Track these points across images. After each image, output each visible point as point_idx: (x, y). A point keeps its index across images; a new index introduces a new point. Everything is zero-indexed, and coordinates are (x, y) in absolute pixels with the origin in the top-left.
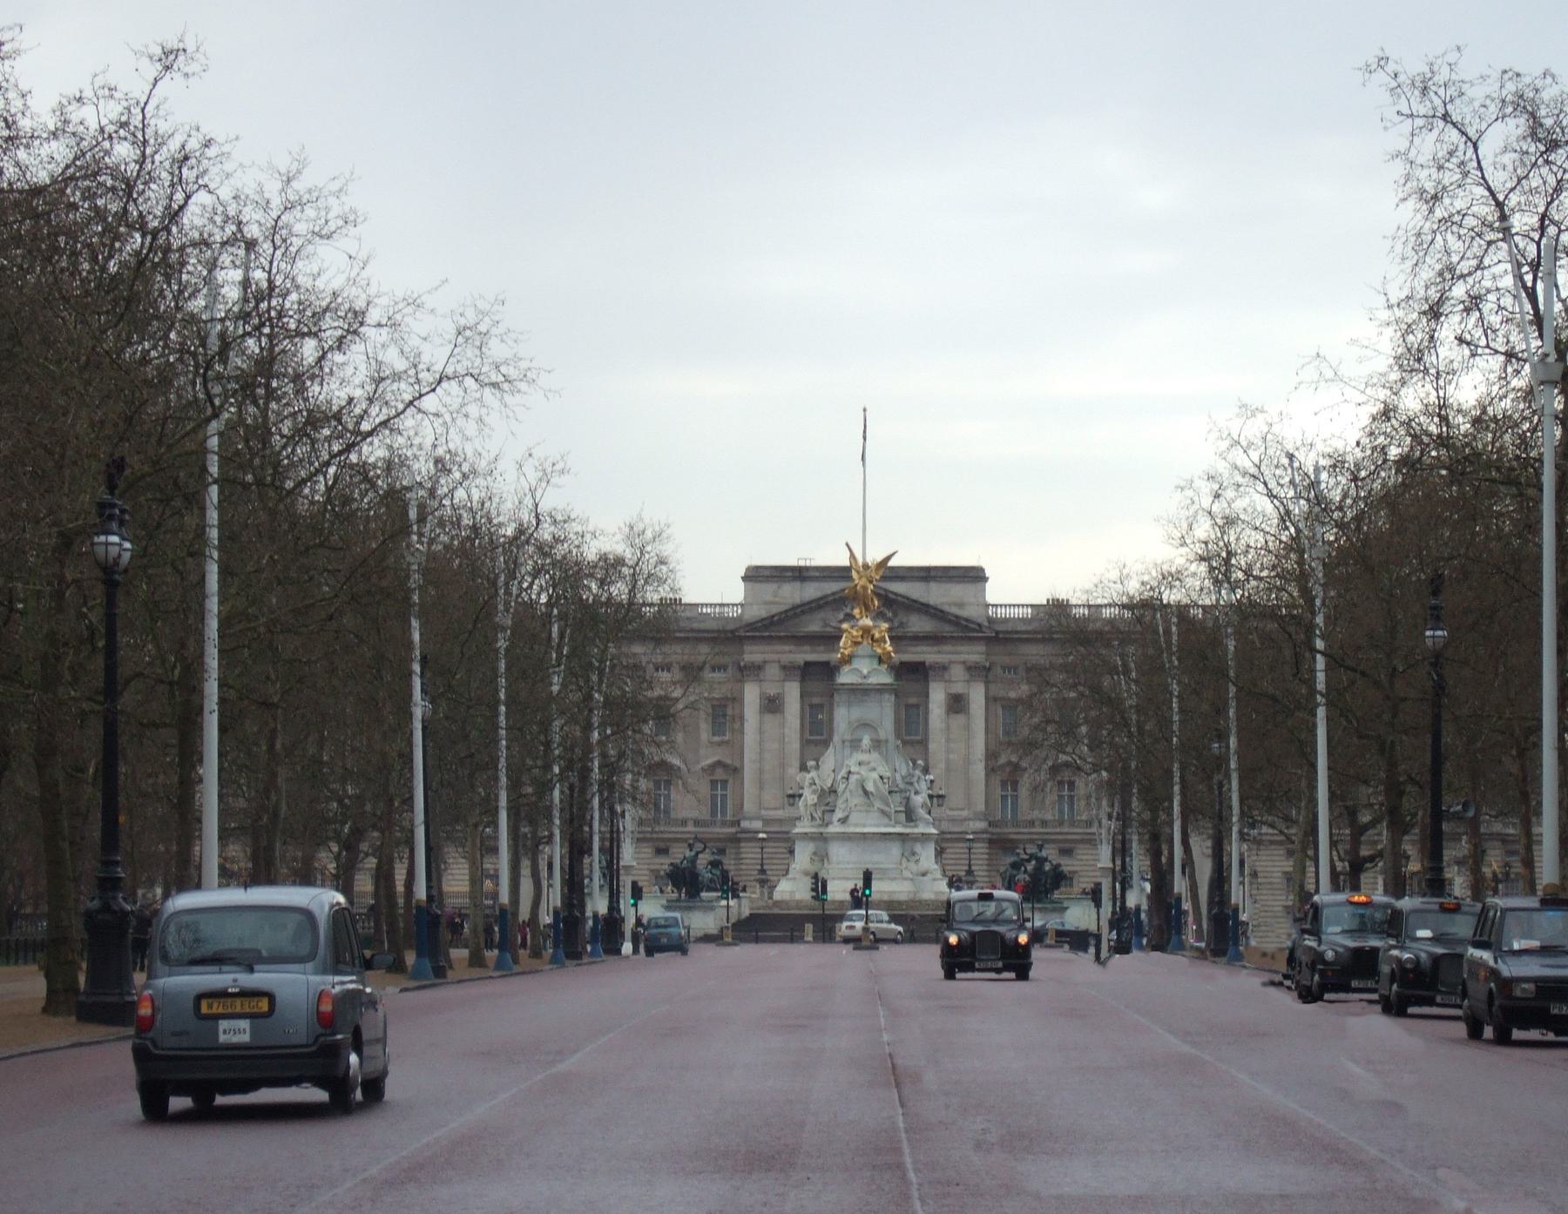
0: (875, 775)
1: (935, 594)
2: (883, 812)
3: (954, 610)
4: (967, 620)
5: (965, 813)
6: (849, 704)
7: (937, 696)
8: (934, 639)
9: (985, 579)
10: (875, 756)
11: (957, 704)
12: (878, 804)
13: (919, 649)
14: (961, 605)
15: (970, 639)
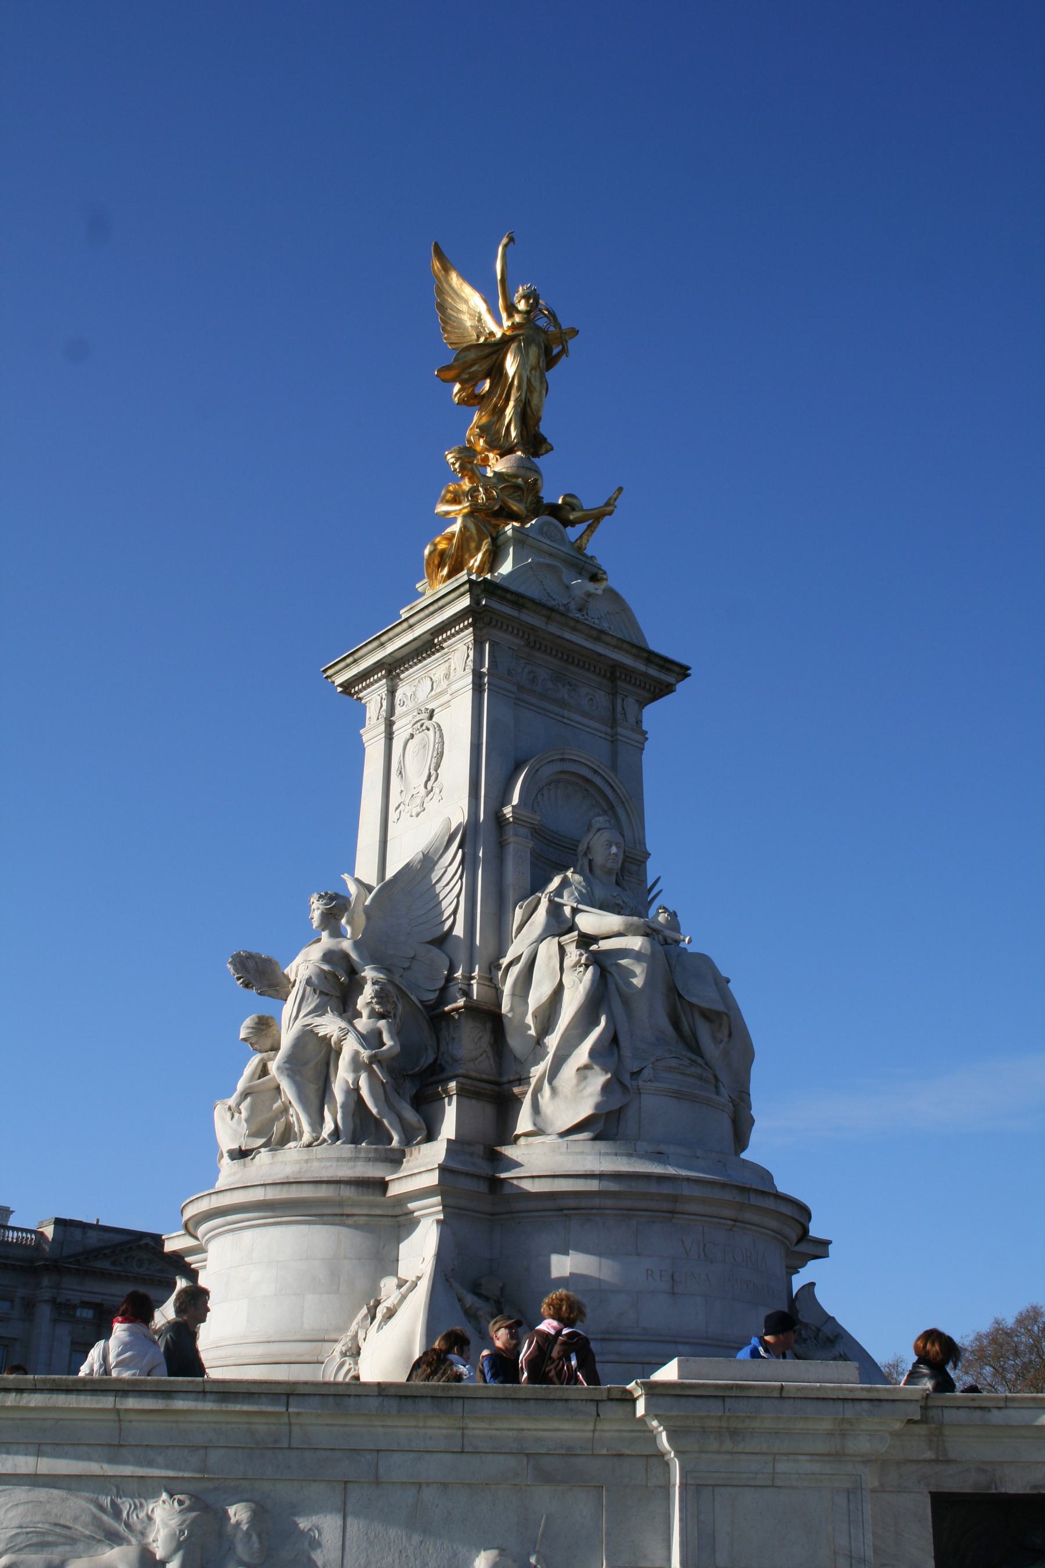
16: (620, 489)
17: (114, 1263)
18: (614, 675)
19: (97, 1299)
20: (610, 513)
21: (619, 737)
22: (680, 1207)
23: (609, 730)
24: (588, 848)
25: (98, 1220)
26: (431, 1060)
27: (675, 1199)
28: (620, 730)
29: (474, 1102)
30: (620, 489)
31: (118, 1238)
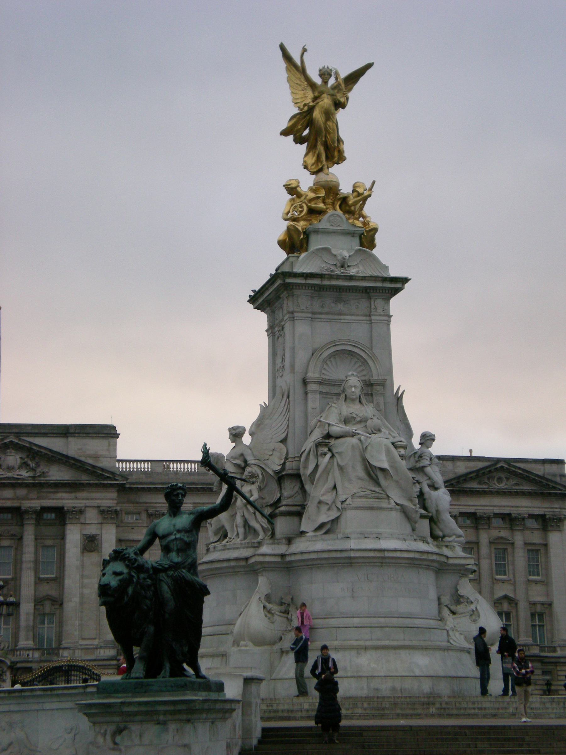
0: (381, 440)
1: (72, 447)
2: (404, 511)
3: (90, 461)
4: (103, 470)
5: (96, 642)
6: (314, 316)
7: (74, 536)
8: (72, 487)
9: (117, 436)
10: (368, 410)
11: (91, 543)
12: (396, 496)
13: (59, 495)
14: (96, 457)
15: (105, 486)
16: (374, 183)
17: (480, 483)
18: (367, 291)
19: (471, 510)
20: (369, 196)
21: (373, 321)
22: (353, 561)
23: (368, 318)
24: (344, 389)
25: (471, 451)
26: (278, 498)
27: (350, 558)
28: (373, 318)
29: (288, 517)
30: (374, 183)
31: (480, 465)
